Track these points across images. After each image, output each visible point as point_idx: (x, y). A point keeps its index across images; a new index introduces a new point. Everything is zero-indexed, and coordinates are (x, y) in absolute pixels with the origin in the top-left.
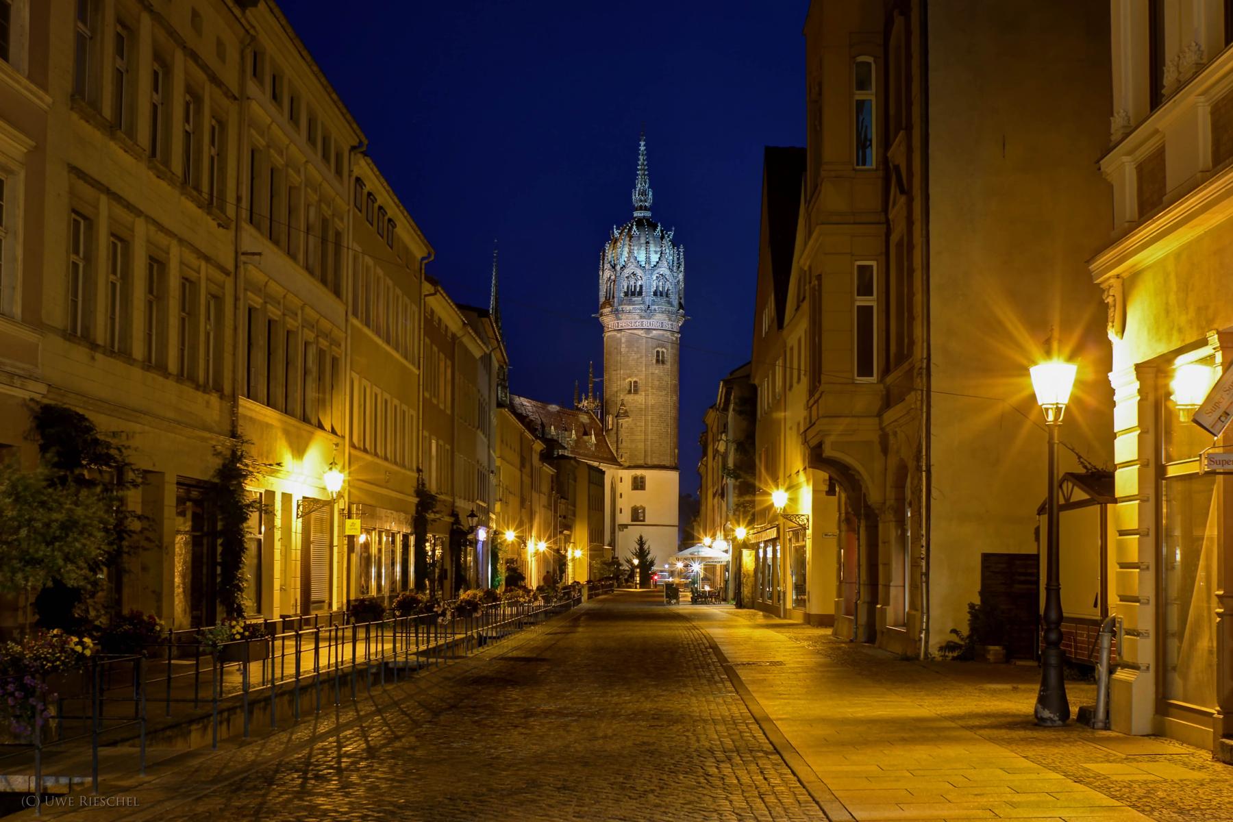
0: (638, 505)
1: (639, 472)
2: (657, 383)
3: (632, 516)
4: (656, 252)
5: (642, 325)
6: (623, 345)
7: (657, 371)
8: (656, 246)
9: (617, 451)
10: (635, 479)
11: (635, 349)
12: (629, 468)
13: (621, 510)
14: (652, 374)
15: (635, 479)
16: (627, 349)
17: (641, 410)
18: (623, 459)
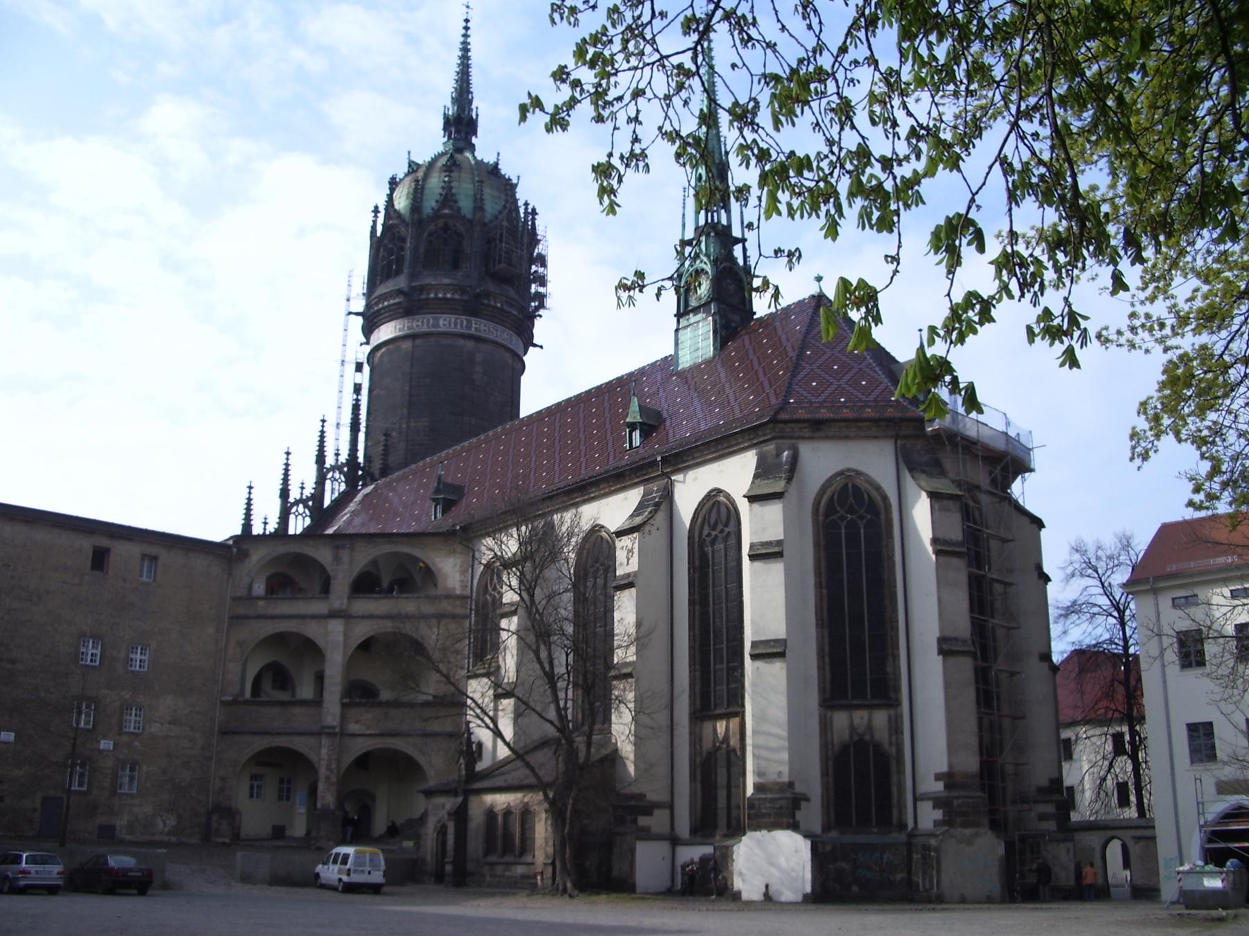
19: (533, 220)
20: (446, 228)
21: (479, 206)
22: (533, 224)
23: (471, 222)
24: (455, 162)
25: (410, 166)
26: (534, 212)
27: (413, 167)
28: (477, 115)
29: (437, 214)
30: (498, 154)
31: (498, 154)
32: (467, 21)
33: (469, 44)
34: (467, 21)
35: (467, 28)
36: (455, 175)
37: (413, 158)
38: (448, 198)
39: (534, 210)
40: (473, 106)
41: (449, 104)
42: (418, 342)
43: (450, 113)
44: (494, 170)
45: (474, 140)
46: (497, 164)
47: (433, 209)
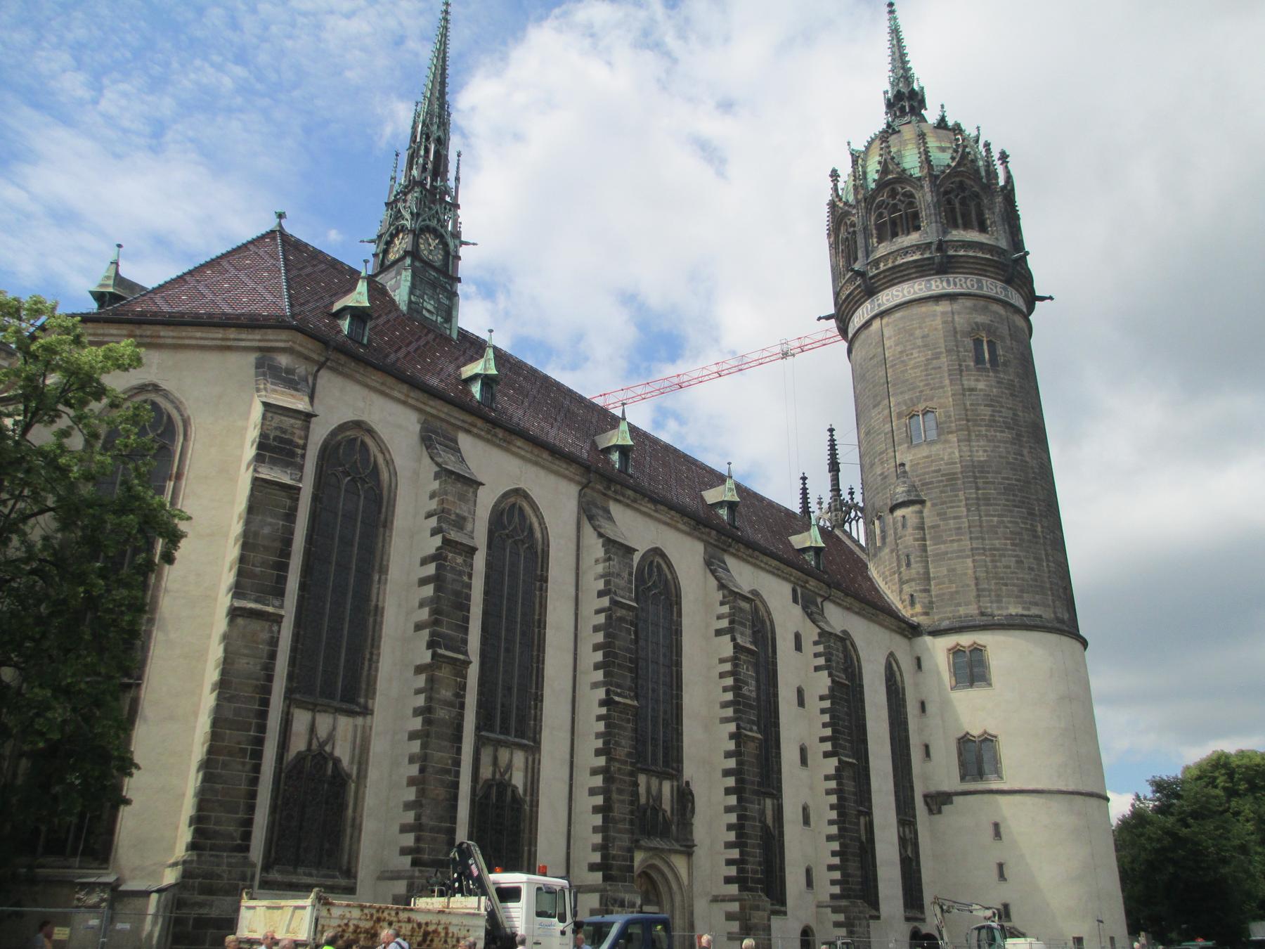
0: (976, 732)
1: (965, 640)
2: (986, 411)
3: (963, 764)
4: (943, 150)
5: (929, 289)
6: (887, 343)
7: (981, 385)
8: (940, 139)
9: (901, 591)
10: (956, 652)
11: (919, 342)
12: (936, 633)
13: (927, 747)
14: (971, 390)
15: (956, 652)
16: (899, 349)
17: (952, 478)
18: (918, 608)
20: (893, 194)
21: (927, 160)
23: (919, 179)
24: (894, 129)
25: (852, 155)
27: (855, 158)
28: (923, 88)
29: (881, 185)
30: (942, 106)
31: (942, 106)
35: (891, 12)
36: (893, 139)
37: (853, 146)
41: (888, 87)
42: (885, 320)
43: (890, 95)
45: (923, 112)
46: (943, 119)
47: (875, 181)
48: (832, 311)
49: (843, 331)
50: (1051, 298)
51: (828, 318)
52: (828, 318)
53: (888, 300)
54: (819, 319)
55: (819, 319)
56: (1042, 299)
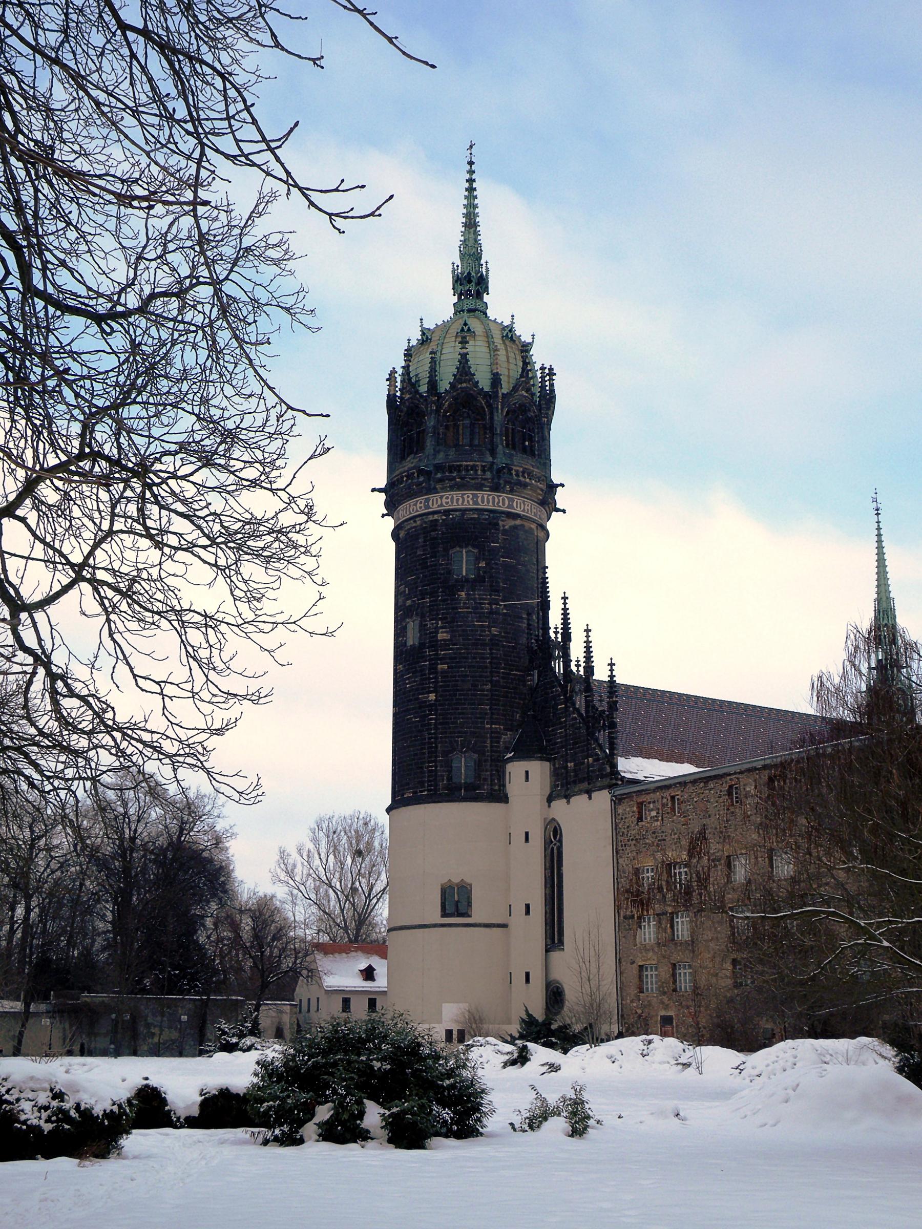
19: (551, 380)
22: (552, 385)
25: (423, 334)
26: (551, 373)
28: (487, 270)
30: (513, 316)
31: (513, 316)
32: (471, 163)
33: (475, 189)
34: (471, 163)
35: (471, 172)
38: (464, 370)
39: (551, 369)
40: (483, 262)
41: (458, 262)
44: (508, 333)
48: (382, 483)
49: (391, 507)
50: (564, 511)
51: (380, 490)
52: (380, 490)
53: (447, 503)
54: (373, 490)
55: (373, 490)
56: (558, 510)
